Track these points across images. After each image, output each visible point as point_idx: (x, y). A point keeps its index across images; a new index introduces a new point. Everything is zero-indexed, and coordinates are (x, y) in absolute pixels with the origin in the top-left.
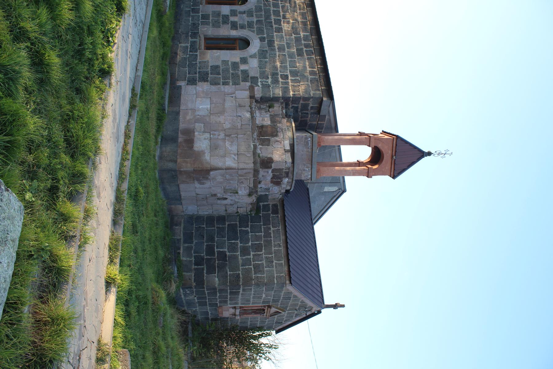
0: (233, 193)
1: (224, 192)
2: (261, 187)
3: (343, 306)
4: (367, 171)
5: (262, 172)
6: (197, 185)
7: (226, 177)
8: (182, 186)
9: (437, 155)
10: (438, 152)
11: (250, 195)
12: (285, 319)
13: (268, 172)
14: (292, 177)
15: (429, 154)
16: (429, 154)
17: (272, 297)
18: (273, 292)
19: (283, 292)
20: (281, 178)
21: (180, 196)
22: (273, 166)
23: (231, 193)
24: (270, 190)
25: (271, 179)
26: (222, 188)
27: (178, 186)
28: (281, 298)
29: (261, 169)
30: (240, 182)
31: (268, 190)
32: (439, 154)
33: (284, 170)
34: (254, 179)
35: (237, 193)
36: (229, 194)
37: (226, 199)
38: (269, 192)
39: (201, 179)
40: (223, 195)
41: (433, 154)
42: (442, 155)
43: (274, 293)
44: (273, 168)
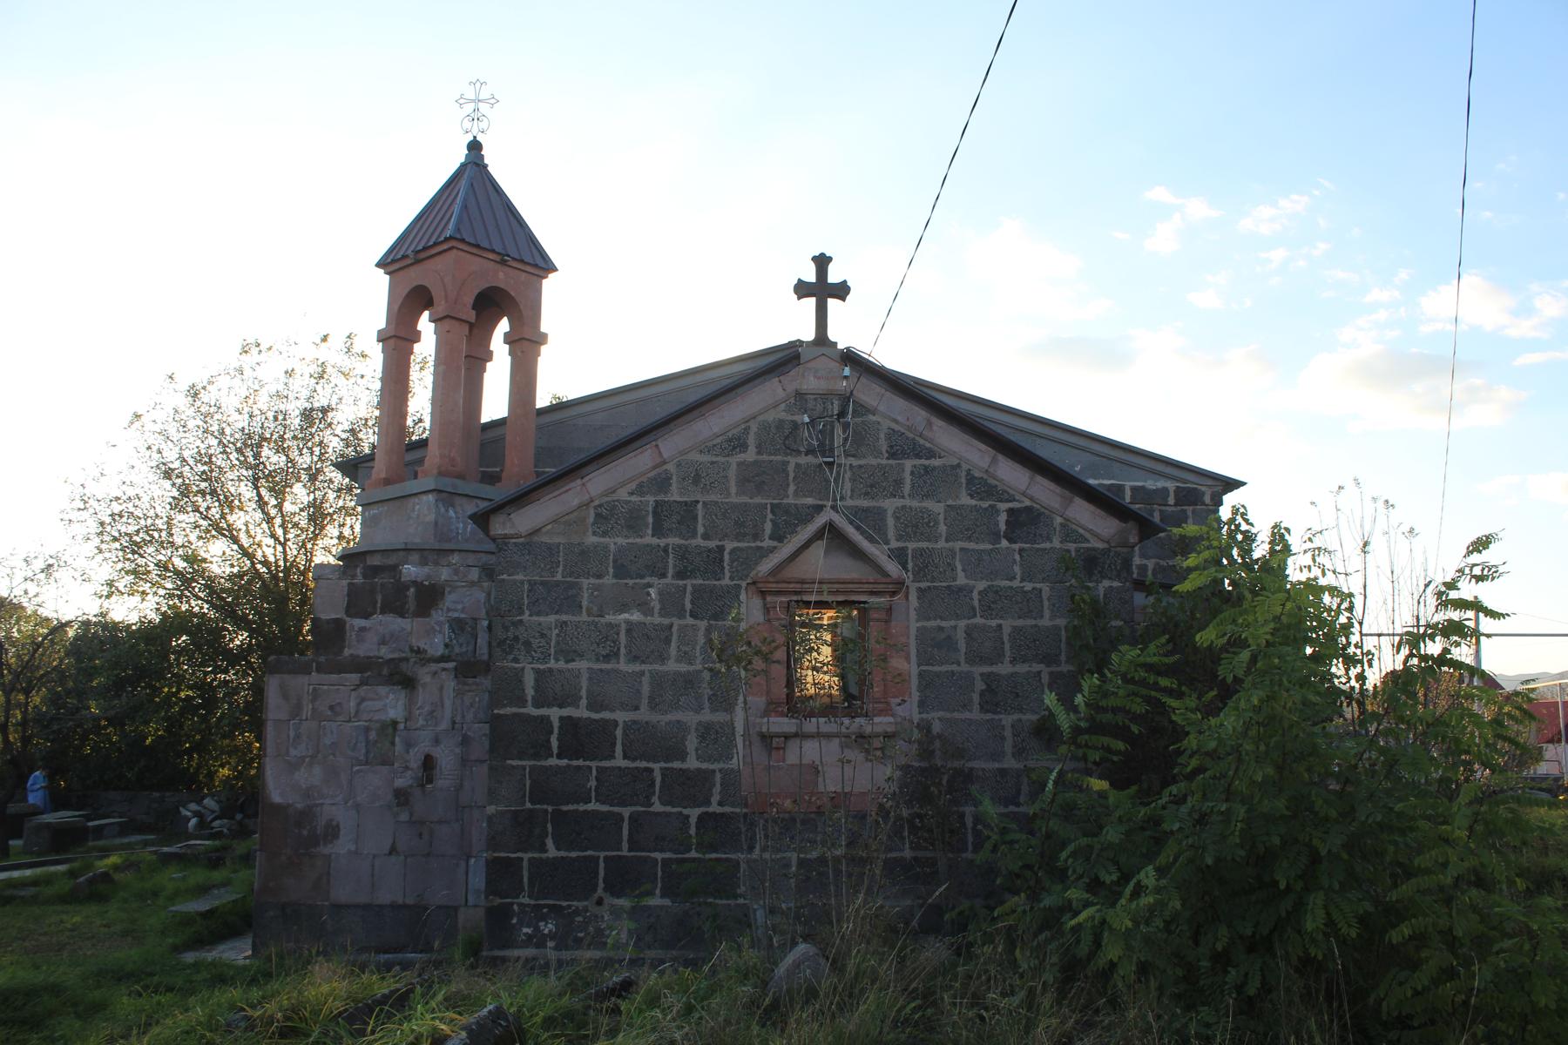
0: (394, 737)
1: (386, 761)
2: (446, 646)
3: (822, 262)
4: (447, 324)
5: (358, 648)
6: (342, 847)
7: (303, 758)
8: (342, 892)
9: (483, 125)
10: (467, 124)
11: (408, 683)
12: (966, 500)
13: (363, 629)
14: (401, 553)
15: (475, 147)
16: (475, 147)
17: (654, 580)
18: (585, 582)
19: (595, 539)
20: (401, 588)
21: (394, 906)
22: (334, 616)
23: (393, 743)
24: (463, 616)
25: (402, 616)
26: (358, 771)
27: (338, 908)
28: (673, 540)
29: (347, 652)
30: (329, 713)
31: (458, 626)
32: (475, 117)
33: (359, 580)
34: (318, 671)
35: (395, 723)
36: (399, 747)
37: (428, 763)
38: (475, 620)
39: (305, 833)
40: (407, 768)
41: (475, 137)
42: (483, 107)
43: (599, 577)
44: (341, 615)
